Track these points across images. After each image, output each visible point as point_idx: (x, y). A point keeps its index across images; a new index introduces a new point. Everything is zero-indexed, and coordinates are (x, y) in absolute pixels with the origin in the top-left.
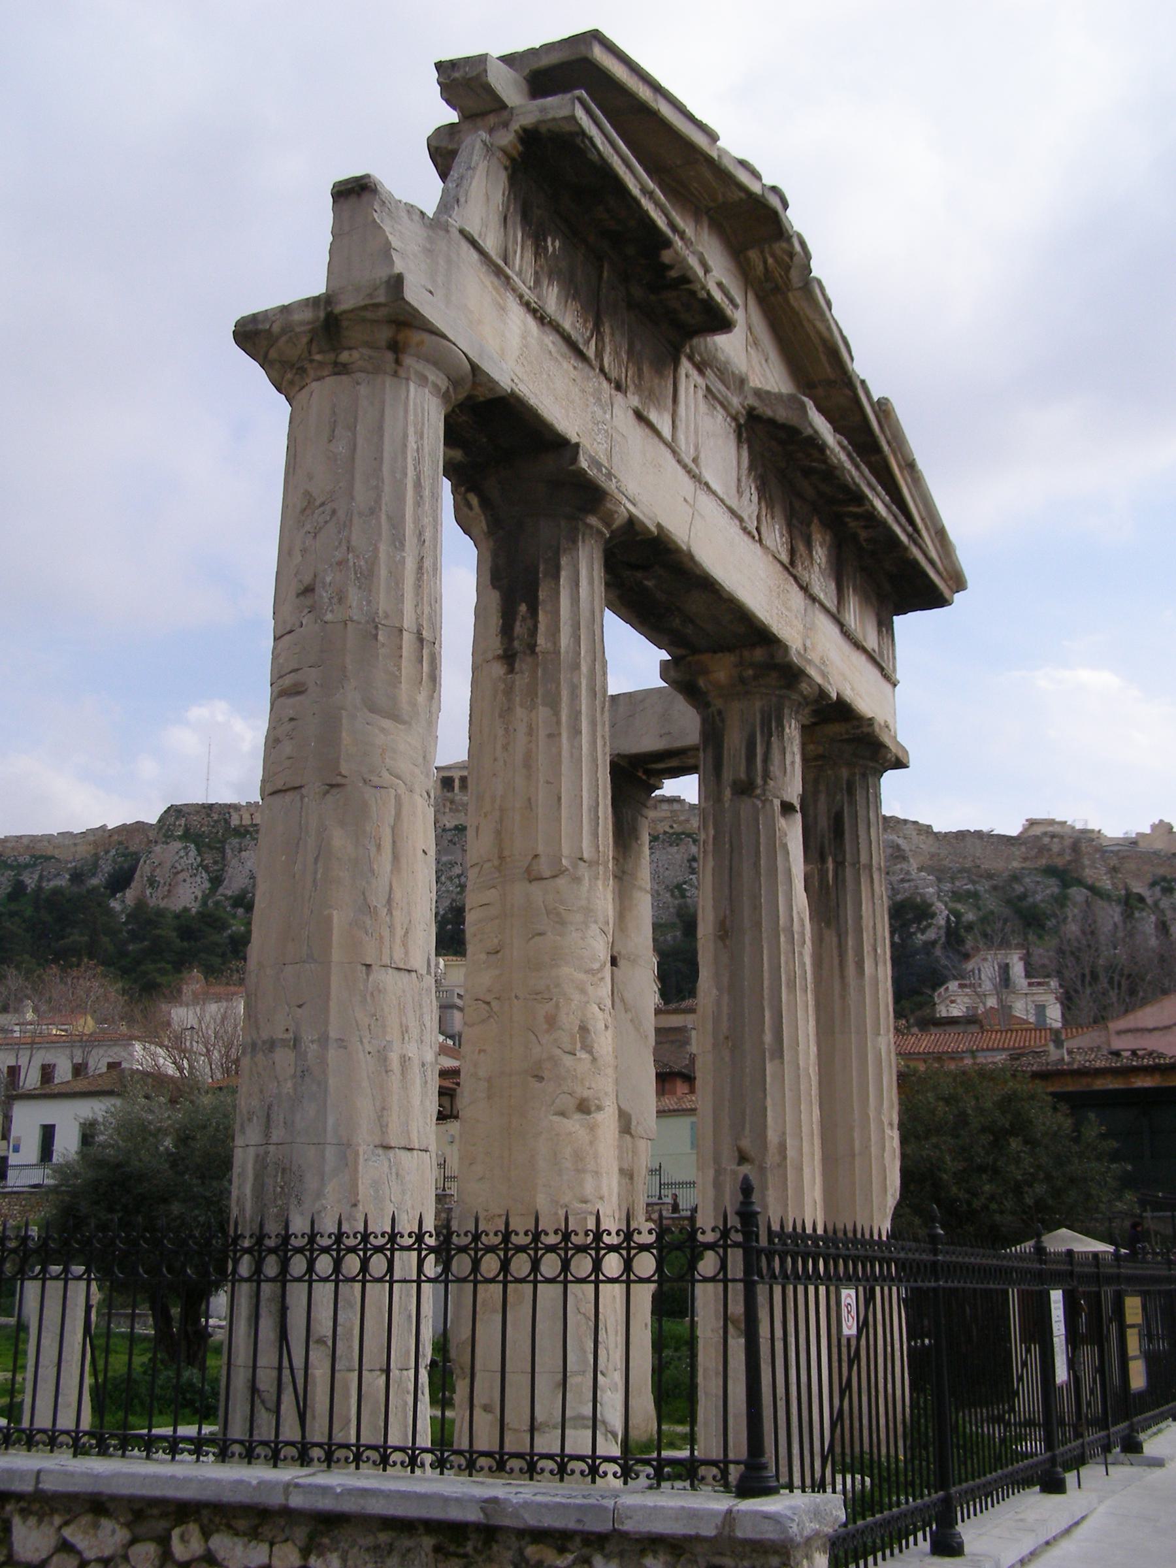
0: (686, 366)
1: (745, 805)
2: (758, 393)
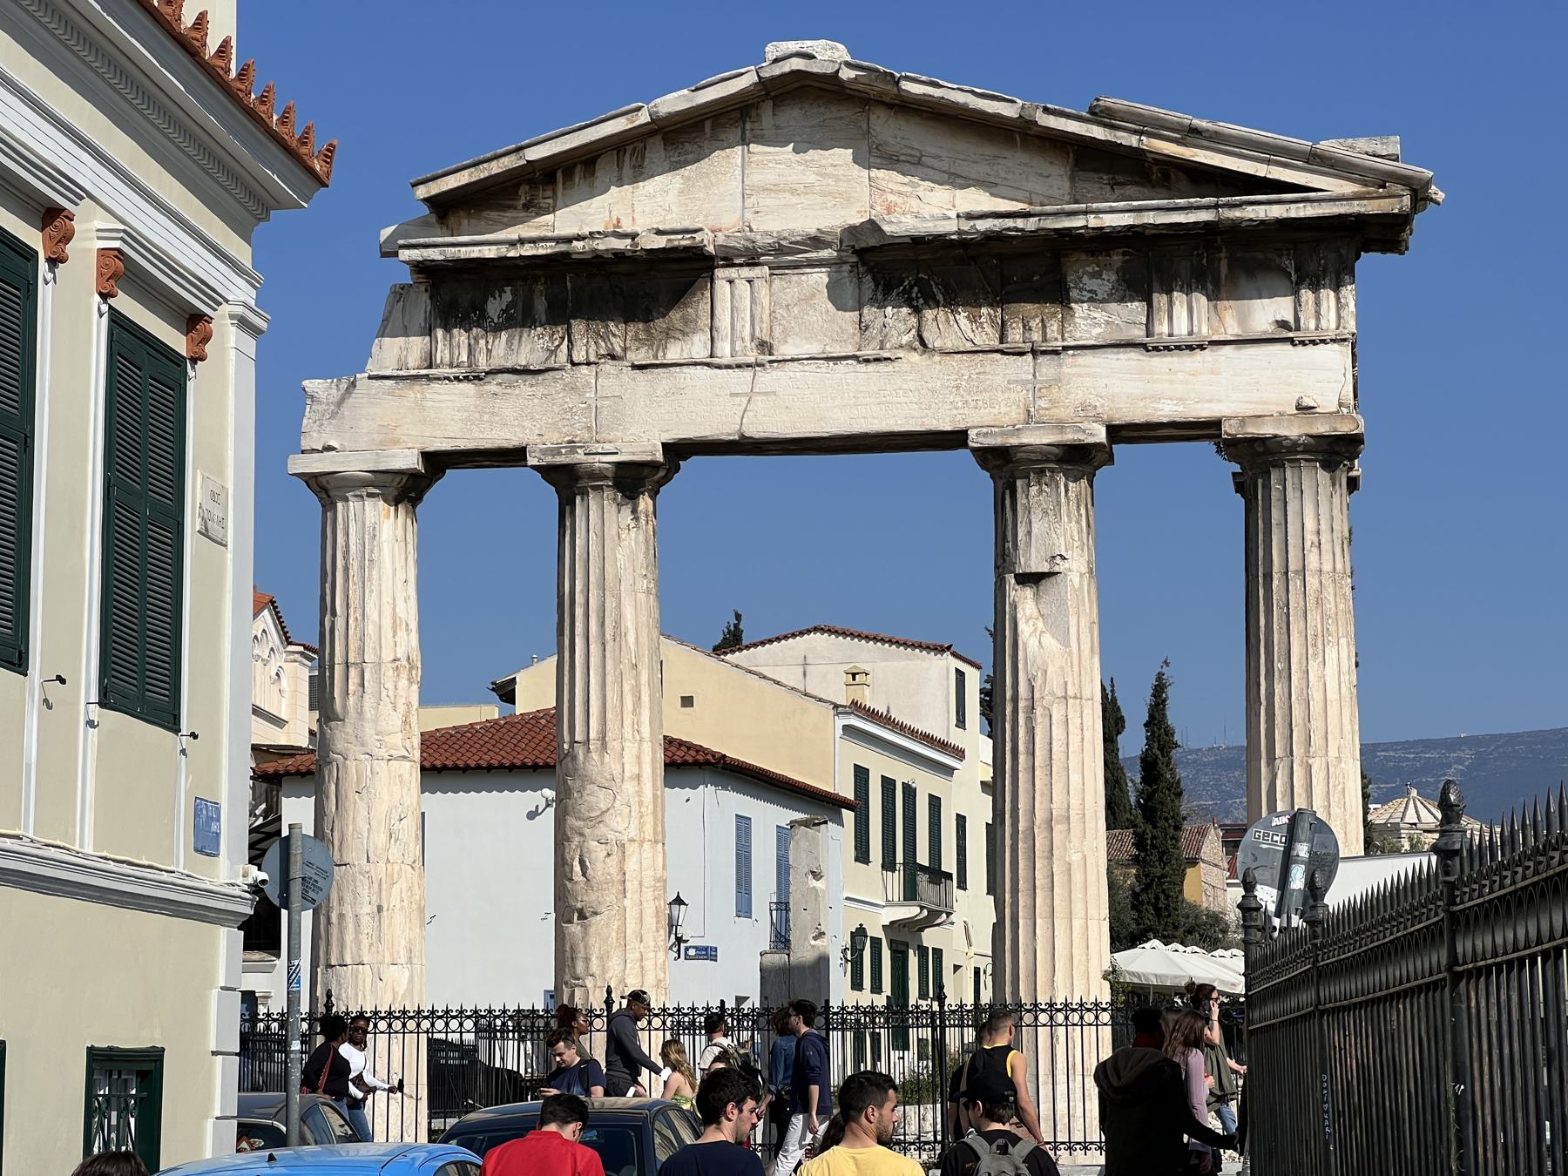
2: (852, 231)
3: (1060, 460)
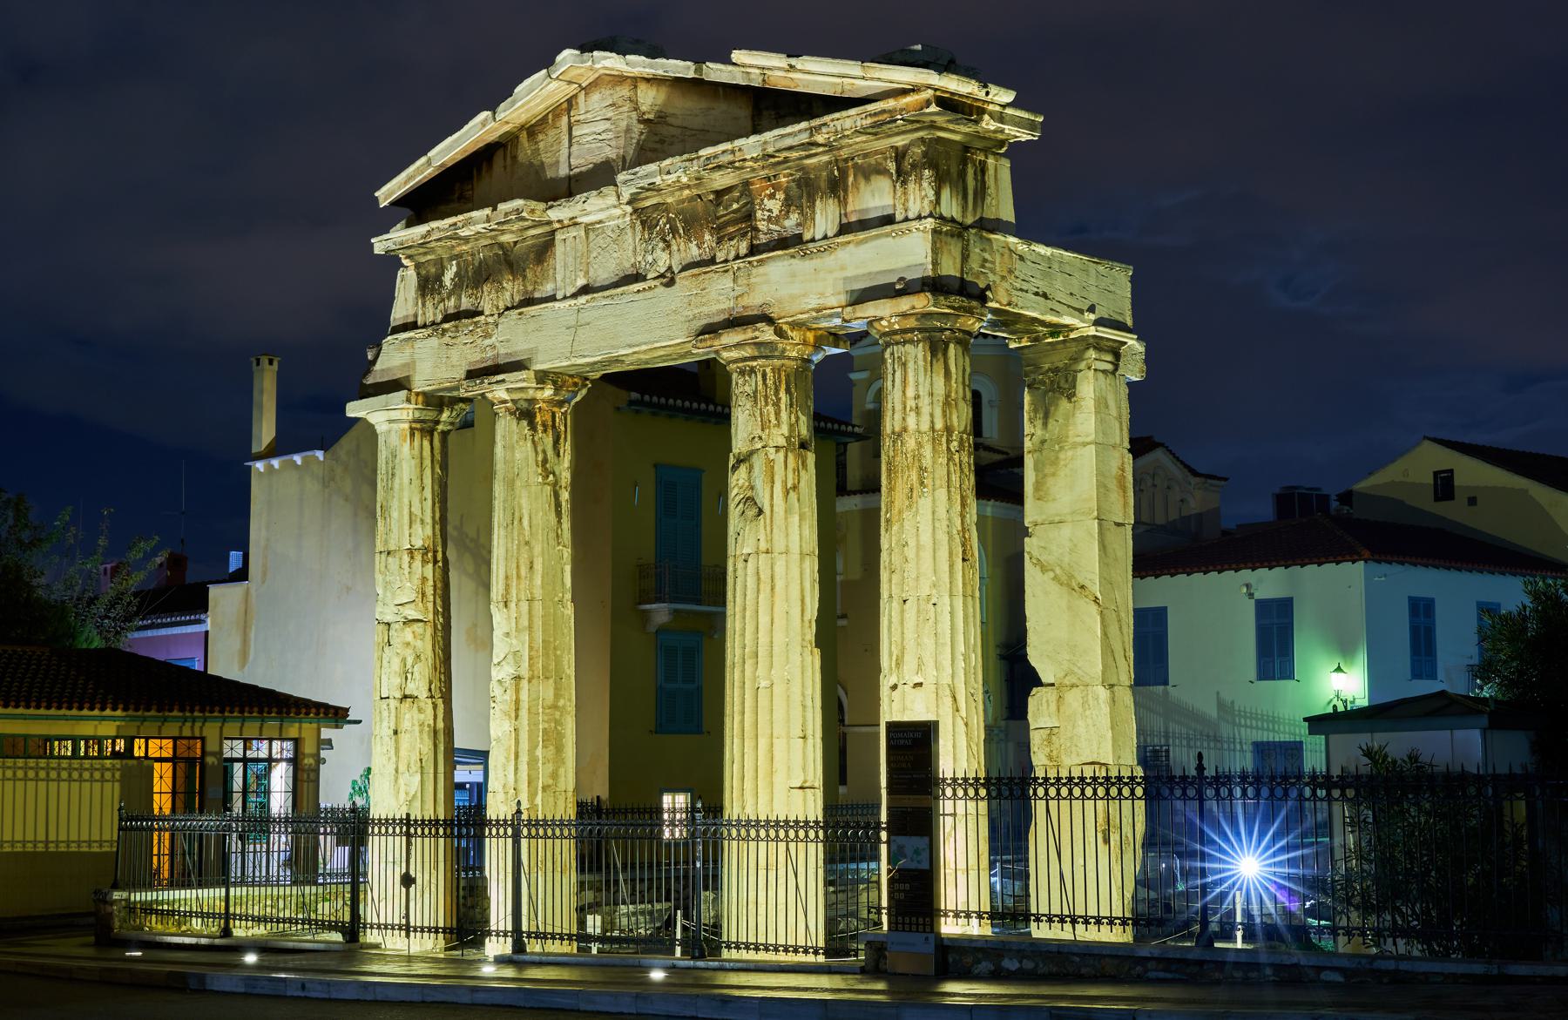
0: (559, 236)
3: (754, 358)
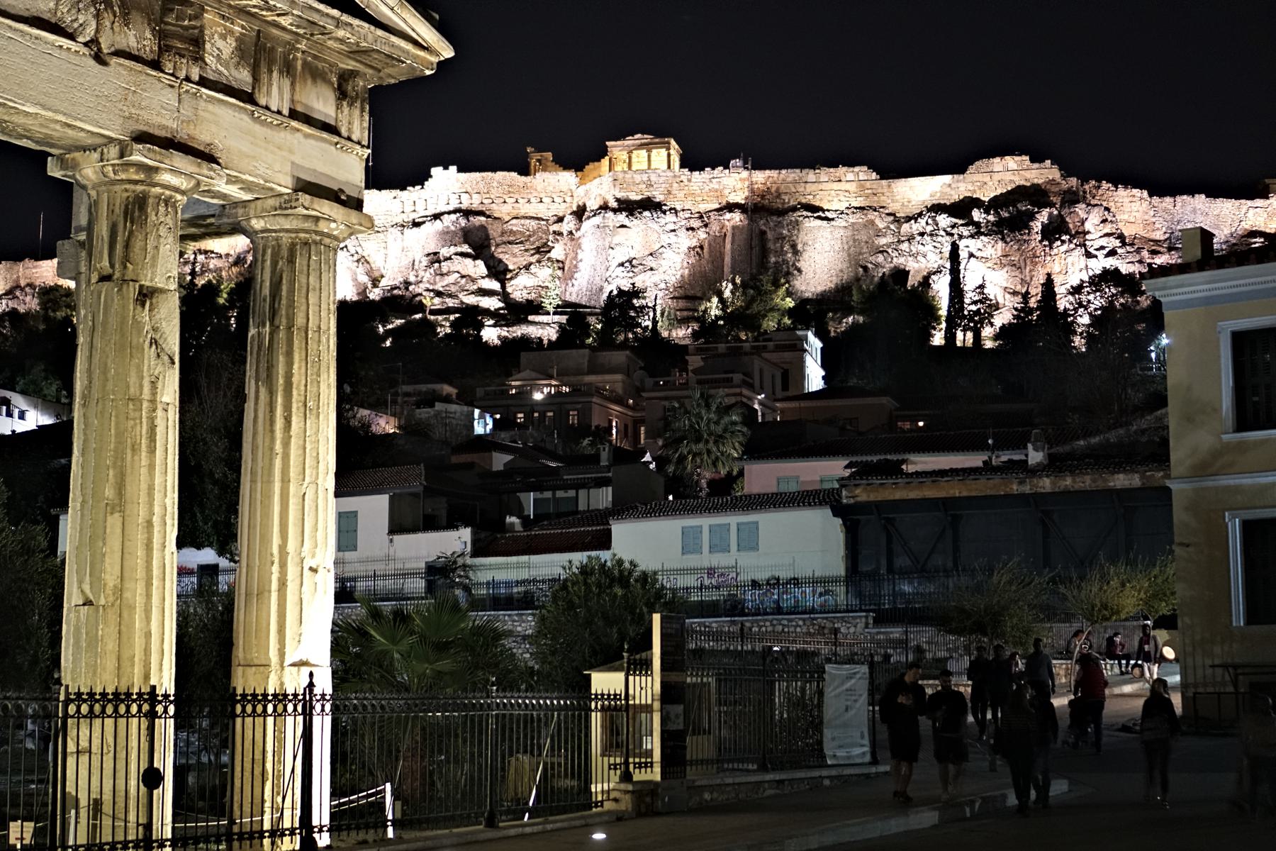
1: (106, 286)
